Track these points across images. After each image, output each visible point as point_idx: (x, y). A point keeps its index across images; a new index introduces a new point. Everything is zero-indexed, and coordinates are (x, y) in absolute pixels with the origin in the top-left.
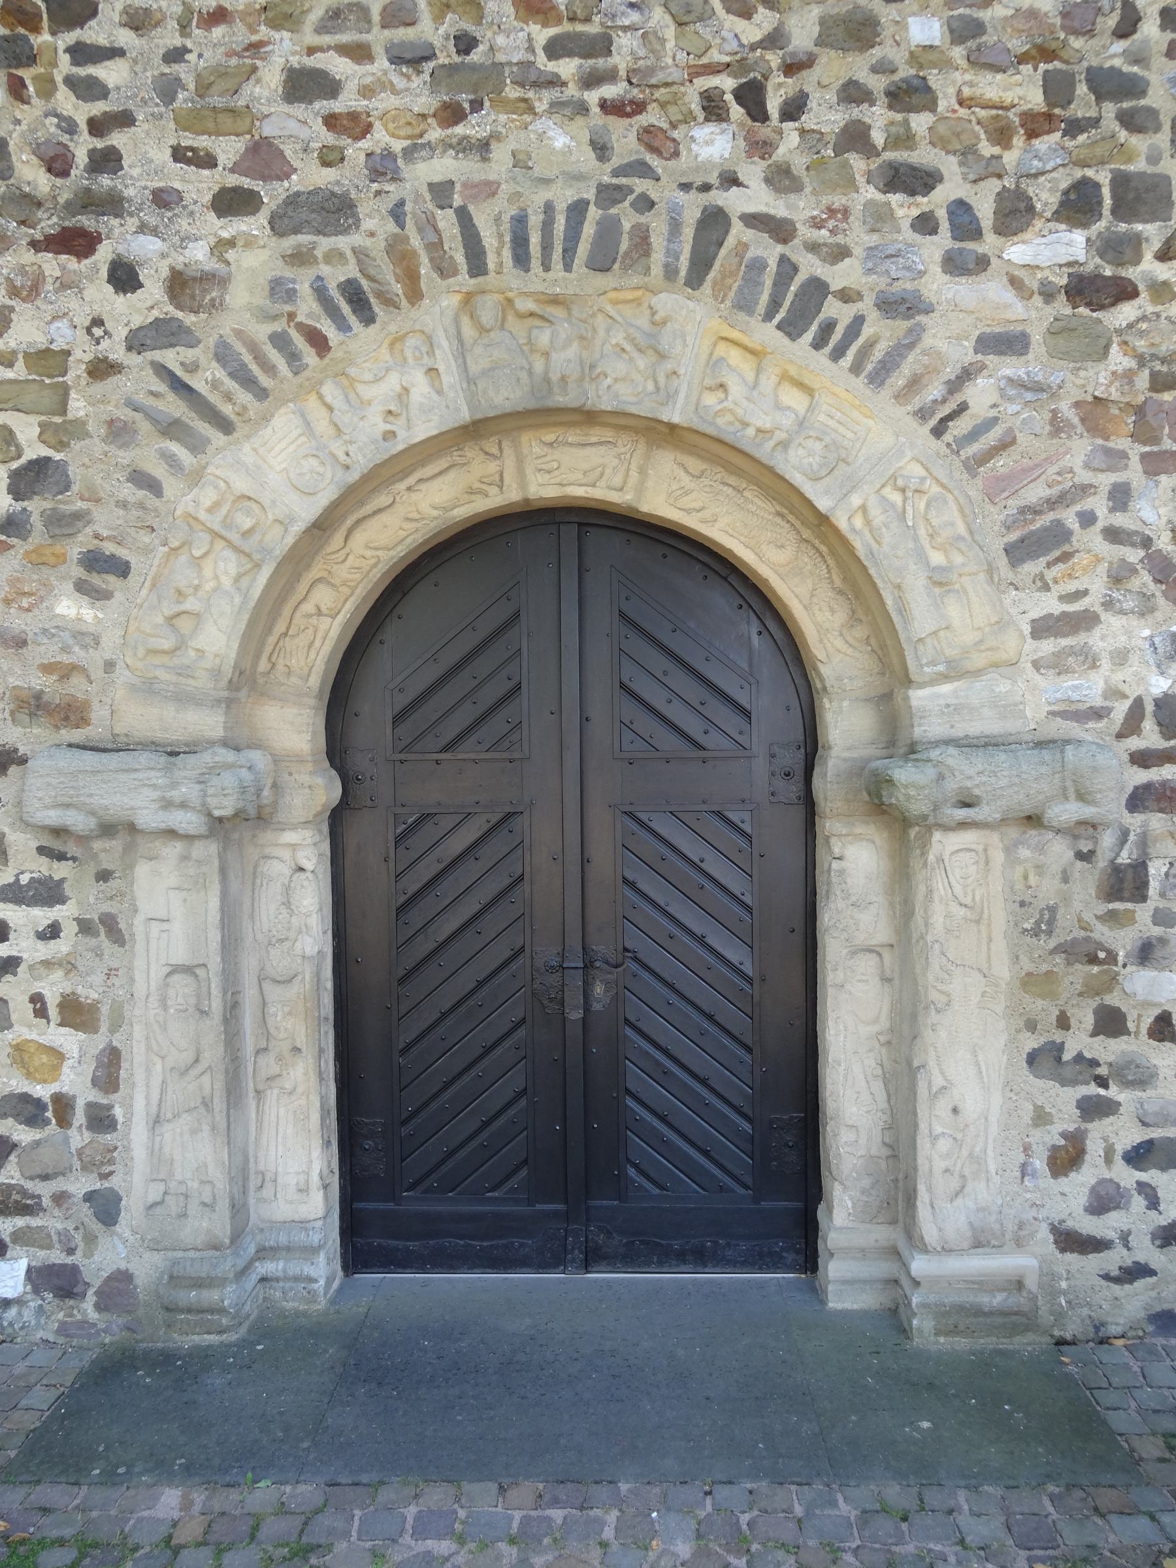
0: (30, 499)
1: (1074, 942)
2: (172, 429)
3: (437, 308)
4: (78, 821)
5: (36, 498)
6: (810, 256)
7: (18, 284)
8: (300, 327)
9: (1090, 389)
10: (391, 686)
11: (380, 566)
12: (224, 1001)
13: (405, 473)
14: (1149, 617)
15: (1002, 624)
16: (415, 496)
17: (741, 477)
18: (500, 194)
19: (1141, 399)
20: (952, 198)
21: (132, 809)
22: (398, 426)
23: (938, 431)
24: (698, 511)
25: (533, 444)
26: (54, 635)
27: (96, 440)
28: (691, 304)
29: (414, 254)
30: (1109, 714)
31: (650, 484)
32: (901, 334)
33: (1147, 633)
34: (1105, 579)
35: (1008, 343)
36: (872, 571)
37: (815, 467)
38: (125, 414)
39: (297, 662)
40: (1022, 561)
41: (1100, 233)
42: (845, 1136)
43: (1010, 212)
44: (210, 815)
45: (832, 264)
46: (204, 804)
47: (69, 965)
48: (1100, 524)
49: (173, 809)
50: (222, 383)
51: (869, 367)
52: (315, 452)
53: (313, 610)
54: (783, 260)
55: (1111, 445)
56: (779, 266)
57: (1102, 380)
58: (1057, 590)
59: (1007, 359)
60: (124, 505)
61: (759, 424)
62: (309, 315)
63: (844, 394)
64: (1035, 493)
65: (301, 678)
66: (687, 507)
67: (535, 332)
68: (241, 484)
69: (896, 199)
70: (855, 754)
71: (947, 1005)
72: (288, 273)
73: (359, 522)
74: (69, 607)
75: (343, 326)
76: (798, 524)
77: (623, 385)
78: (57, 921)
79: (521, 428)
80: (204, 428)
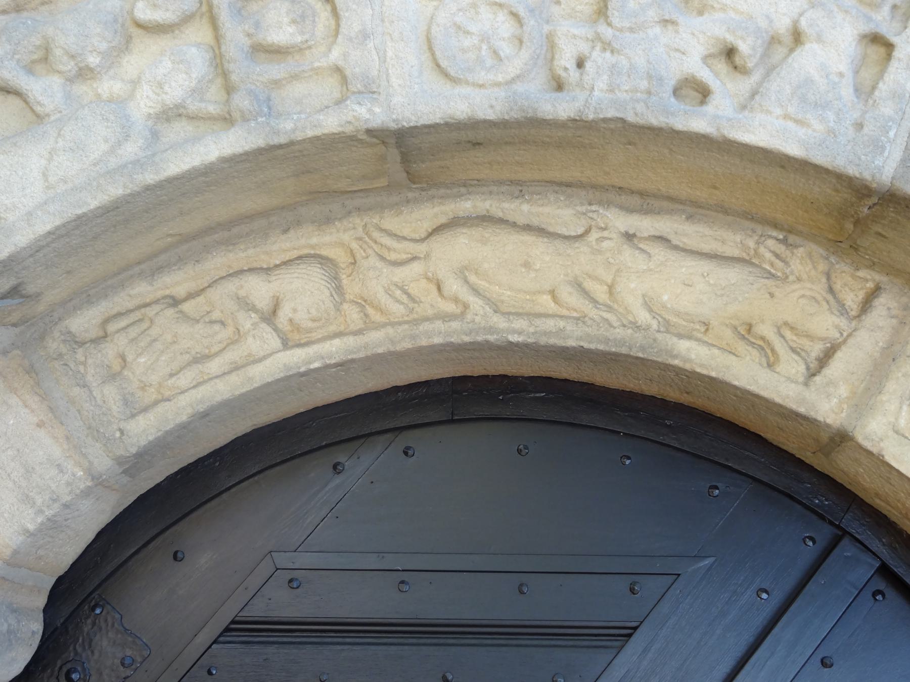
10: (282, 560)
11: (455, 325)
16: (628, 255)
39: (147, 367)
52: (522, 12)
65: (126, 402)
73: (486, 219)
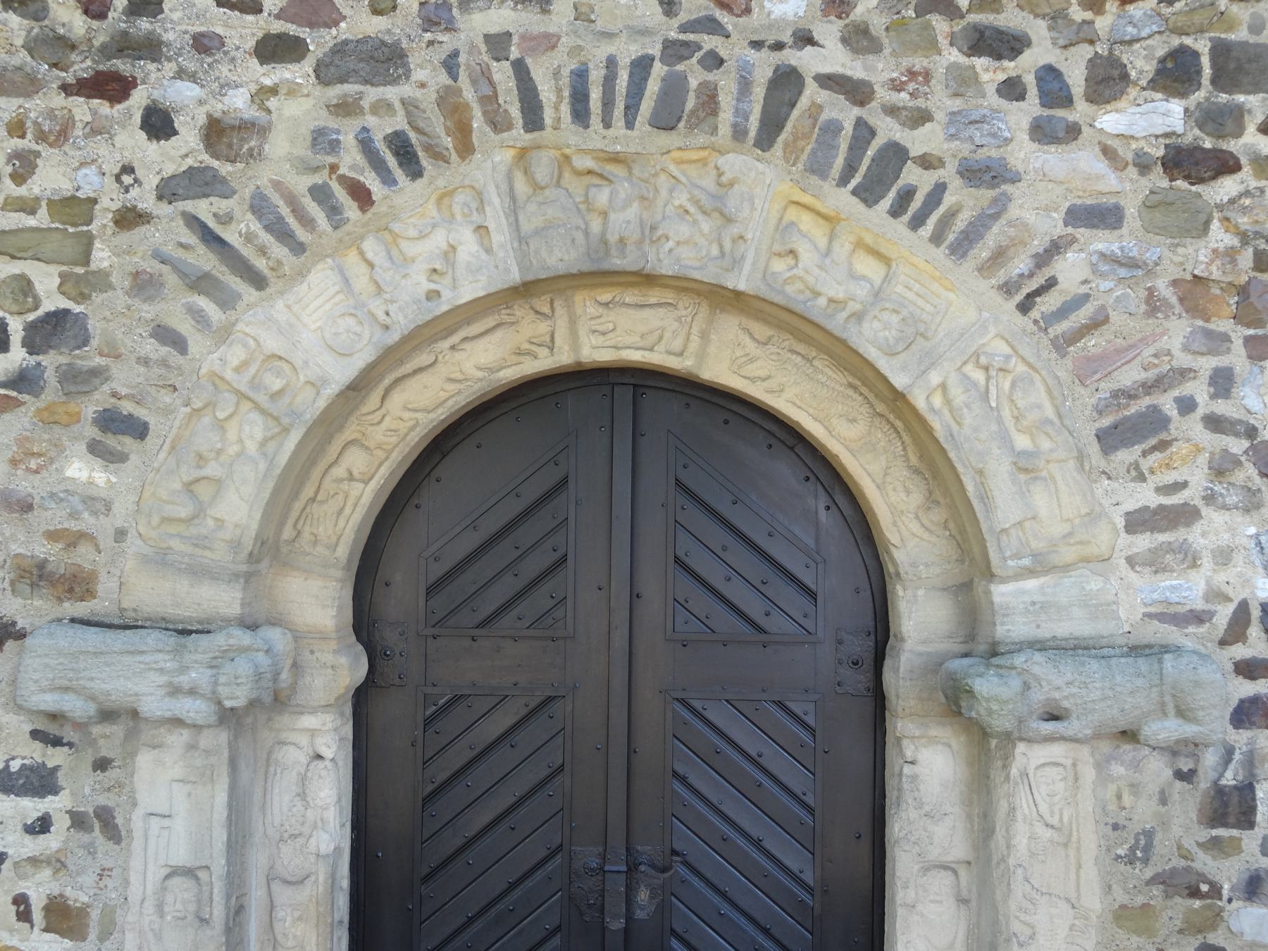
0: (45, 352)
1: (1174, 871)
2: (201, 283)
3: (489, 164)
4: (75, 706)
5: (52, 352)
6: (888, 119)
7: (46, 128)
8: (343, 180)
9: (1189, 268)
11: (418, 429)
12: (227, 907)
13: (450, 332)
14: (1255, 514)
15: (1093, 517)
16: (458, 356)
17: (810, 345)
18: (560, 47)
19: (1244, 279)
20: (1041, 64)
21: (136, 695)
22: (443, 286)
23: (1024, 307)
24: (764, 380)
25: (588, 303)
26: (62, 500)
27: (120, 292)
28: (760, 166)
29: (467, 106)
30: (1211, 619)
31: (712, 349)
32: (986, 204)
33: (1252, 530)
34: (1206, 471)
35: (1102, 216)
36: (952, 455)
37: (892, 341)
38: (152, 266)
39: (325, 530)
40: (1116, 448)
41: (1199, 104)
43: (1103, 80)
44: (219, 703)
45: (913, 128)
46: (214, 692)
47: (57, 863)
48: (1200, 411)
49: (180, 696)
50: (257, 236)
51: (951, 237)
53: (345, 475)
54: (860, 123)
55: (1212, 326)
56: (855, 129)
57: (1202, 258)
58: (1153, 481)
59: (1100, 233)
60: (145, 361)
61: (831, 294)
62: (352, 168)
63: (922, 265)
64: (1130, 376)
66: (751, 375)
67: (593, 191)
68: (272, 343)
69: (980, 62)
70: (930, 649)
72: (332, 123)
73: (398, 381)
74: (80, 469)
75: (387, 179)
76: (871, 397)
77: (685, 247)
78: (47, 814)
79: (577, 287)
80: (235, 283)
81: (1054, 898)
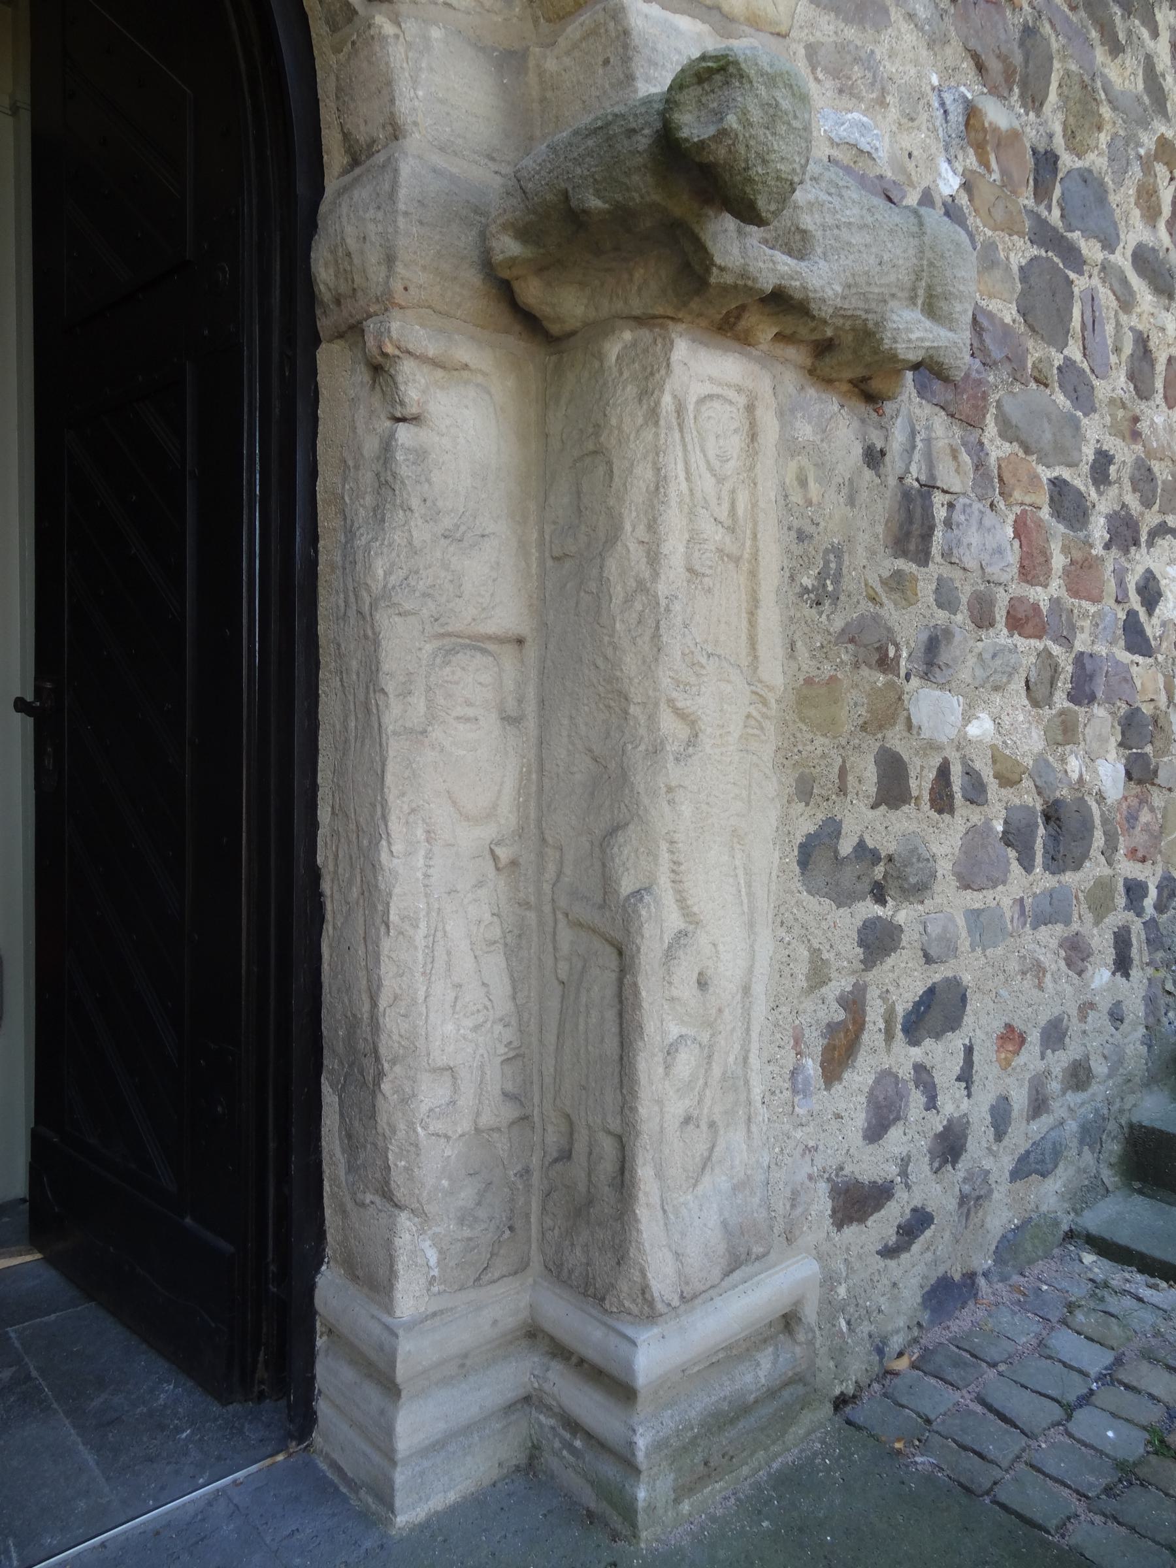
42: (431, 1095)
71: (689, 743)
81: (725, 664)
